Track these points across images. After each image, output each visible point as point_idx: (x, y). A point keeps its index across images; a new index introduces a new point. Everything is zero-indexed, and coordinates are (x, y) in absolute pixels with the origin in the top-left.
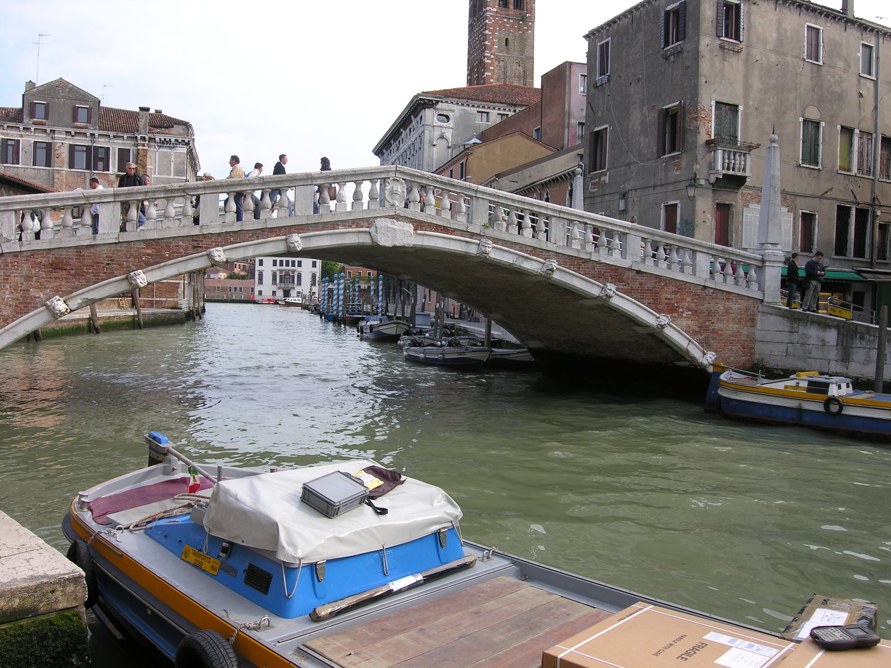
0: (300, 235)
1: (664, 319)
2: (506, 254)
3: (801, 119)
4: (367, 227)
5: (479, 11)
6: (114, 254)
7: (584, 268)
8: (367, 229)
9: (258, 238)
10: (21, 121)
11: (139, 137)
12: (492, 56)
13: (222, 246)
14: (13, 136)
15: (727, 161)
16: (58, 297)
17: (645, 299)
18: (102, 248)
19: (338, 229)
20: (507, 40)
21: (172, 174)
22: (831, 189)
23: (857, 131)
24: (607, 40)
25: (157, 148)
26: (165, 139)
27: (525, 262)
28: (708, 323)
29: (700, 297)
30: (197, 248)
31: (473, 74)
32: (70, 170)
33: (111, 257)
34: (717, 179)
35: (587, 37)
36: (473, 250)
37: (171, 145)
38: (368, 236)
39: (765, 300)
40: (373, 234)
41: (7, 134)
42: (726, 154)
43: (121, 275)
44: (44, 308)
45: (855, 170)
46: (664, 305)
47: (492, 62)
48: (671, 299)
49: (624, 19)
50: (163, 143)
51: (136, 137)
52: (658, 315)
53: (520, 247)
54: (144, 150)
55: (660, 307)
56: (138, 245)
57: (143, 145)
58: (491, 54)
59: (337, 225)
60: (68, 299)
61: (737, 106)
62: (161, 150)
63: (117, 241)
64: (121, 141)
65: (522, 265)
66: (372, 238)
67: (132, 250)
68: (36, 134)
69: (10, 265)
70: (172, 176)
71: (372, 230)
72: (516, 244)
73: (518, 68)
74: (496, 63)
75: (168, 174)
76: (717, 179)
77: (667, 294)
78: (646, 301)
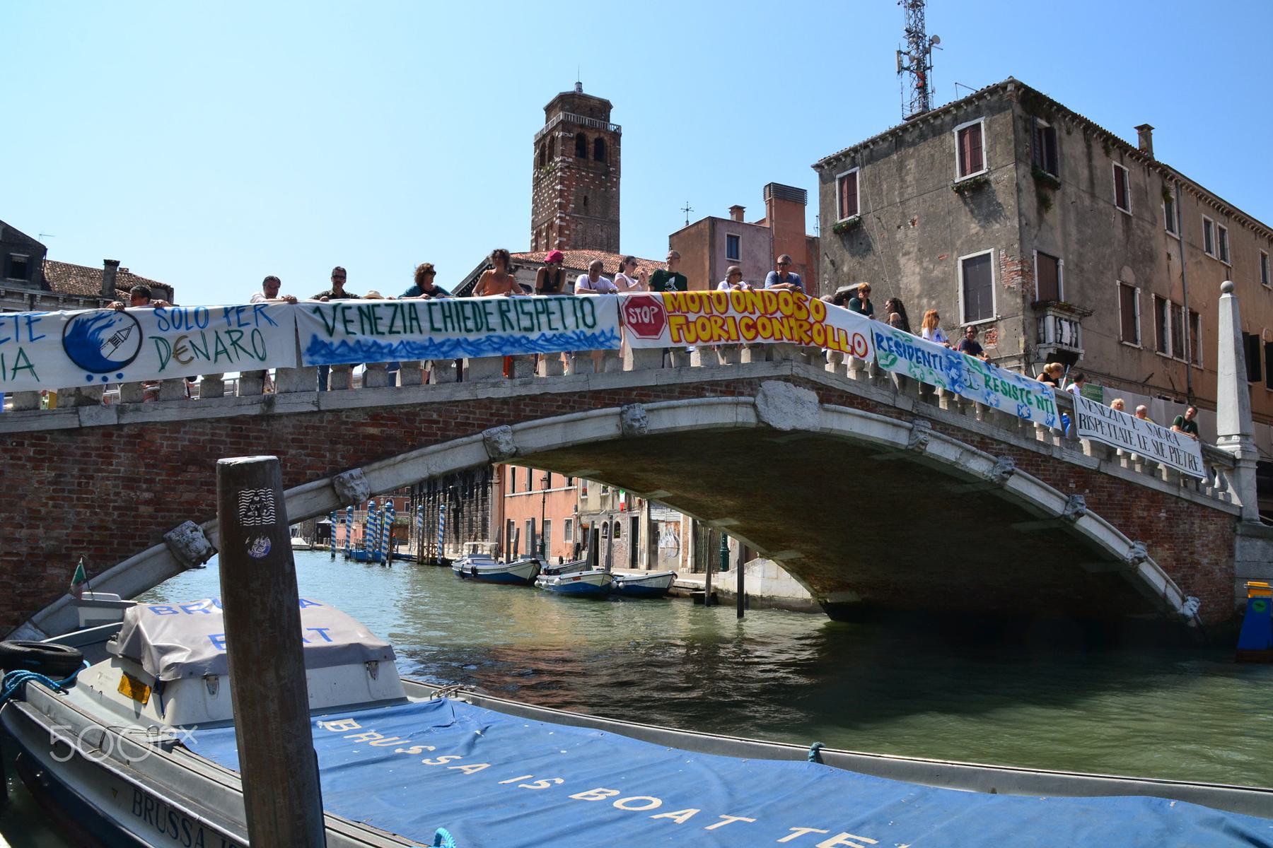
0: (644, 405)
2: (946, 445)
3: (1118, 282)
4: (750, 395)
5: (549, 161)
6: (307, 434)
7: (1044, 470)
8: (751, 399)
9: (573, 410)
12: (568, 218)
13: (511, 423)
15: (1060, 332)
16: (190, 523)
17: (1115, 518)
18: (285, 421)
19: (705, 396)
20: (585, 198)
22: (1151, 376)
23: (1169, 302)
24: (853, 170)
27: (971, 461)
28: (1185, 554)
29: (1174, 515)
30: (464, 429)
31: (539, 239)
33: (301, 441)
34: (1050, 354)
35: (817, 167)
36: (902, 439)
38: (750, 411)
39: (1244, 516)
40: (761, 406)
43: (318, 477)
44: (161, 546)
45: (1170, 353)
46: (1136, 528)
47: (568, 225)
48: (1144, 518)
49: (881, 143)
52: (1132, 543)
53: (964, 435)
55: (1132, 530)
56: (356, 417)
58: (566, 215)
59: (703, 389)
60: (210, 528)
61: (1056, 260)
63: (315, 409)
65: (968, 465)
66: (758, 415)
67: (343, 427)
69: (94, 453)
71: (759, 400)
72: (959, 429)
73: (600, 233)
74: (573, 226)
76: (1050, 354)
78: (1117, 521)
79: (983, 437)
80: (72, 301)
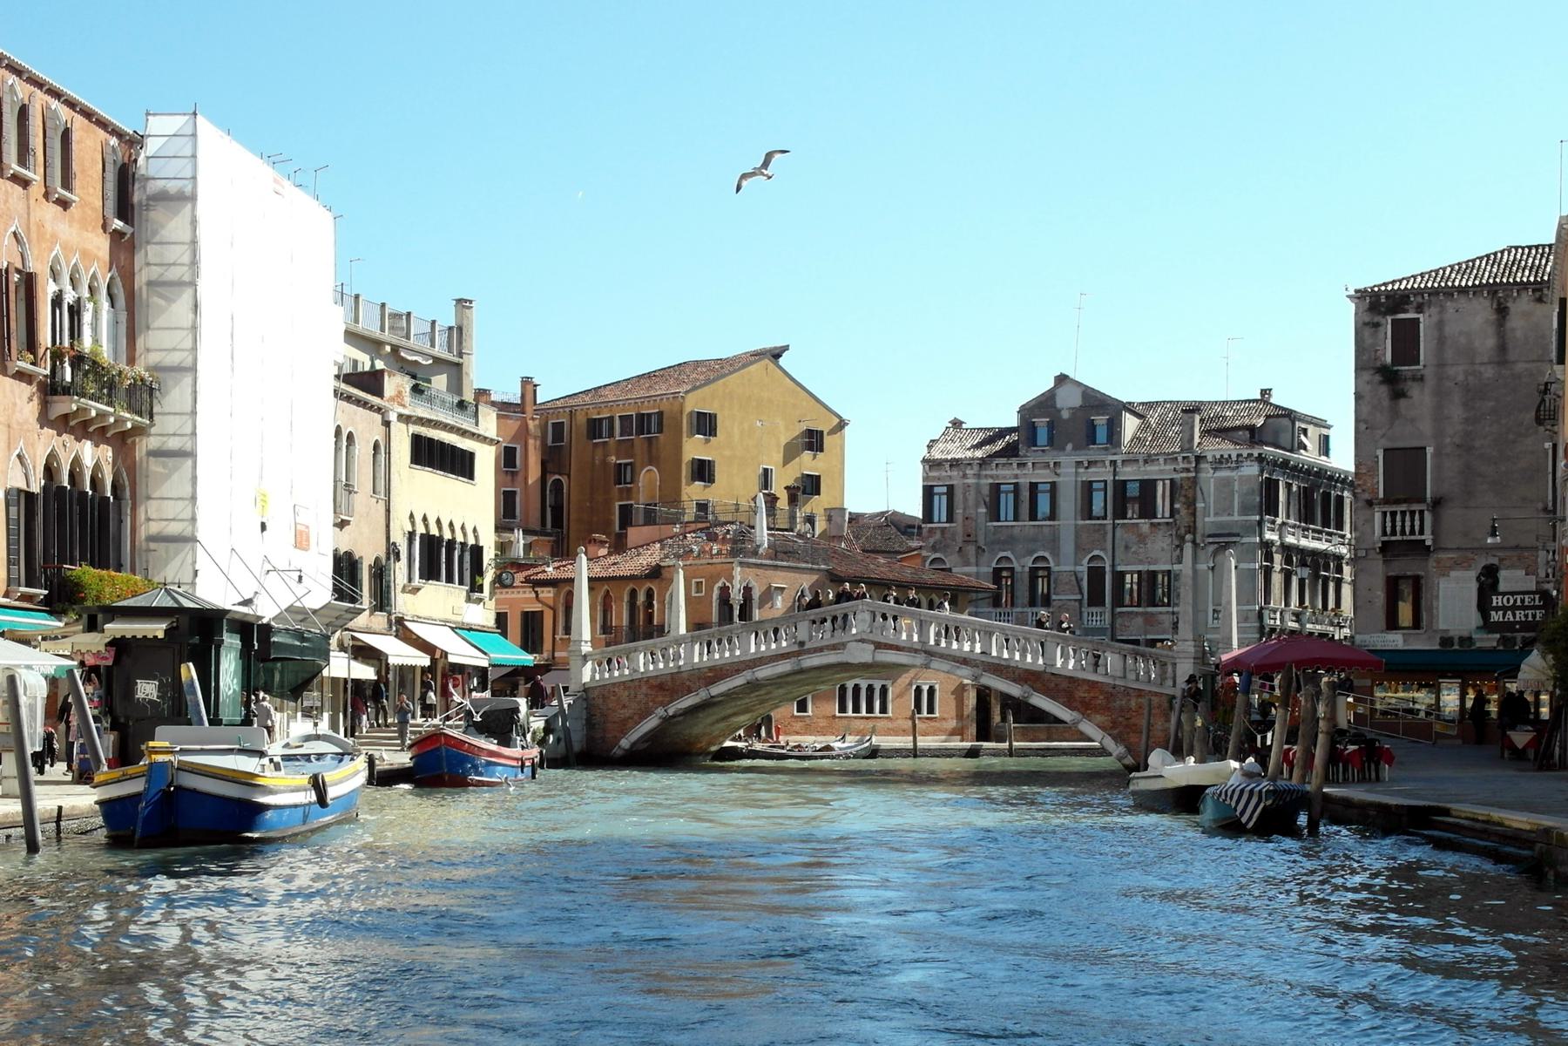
1: (1075, 715)
10: (1017, 455)
11: (1180, 459)
14: (1005, 477)
21: (1236, 514)
25: (1212, 471)
26: (1222, 456)
32: (1083, 522)
37: (1234, 465)
41: (997, 476)
42: (1388, 514)
50: (1221, 463)
51: (1176, 458)
54: (1189, 478)
55: (1075, 704)
56: (706, 670)
57: (1188, 470)
62: (1219, 474)
64: (1157, 468)
68: (1036, 472)
70: (1236, 517)
75: (1229, 515)
77: (1081, 693)
79: (965, 659)
80: (1153, 461)
